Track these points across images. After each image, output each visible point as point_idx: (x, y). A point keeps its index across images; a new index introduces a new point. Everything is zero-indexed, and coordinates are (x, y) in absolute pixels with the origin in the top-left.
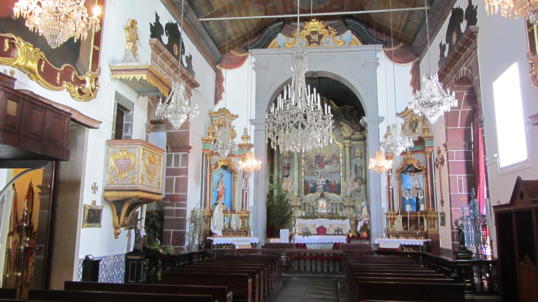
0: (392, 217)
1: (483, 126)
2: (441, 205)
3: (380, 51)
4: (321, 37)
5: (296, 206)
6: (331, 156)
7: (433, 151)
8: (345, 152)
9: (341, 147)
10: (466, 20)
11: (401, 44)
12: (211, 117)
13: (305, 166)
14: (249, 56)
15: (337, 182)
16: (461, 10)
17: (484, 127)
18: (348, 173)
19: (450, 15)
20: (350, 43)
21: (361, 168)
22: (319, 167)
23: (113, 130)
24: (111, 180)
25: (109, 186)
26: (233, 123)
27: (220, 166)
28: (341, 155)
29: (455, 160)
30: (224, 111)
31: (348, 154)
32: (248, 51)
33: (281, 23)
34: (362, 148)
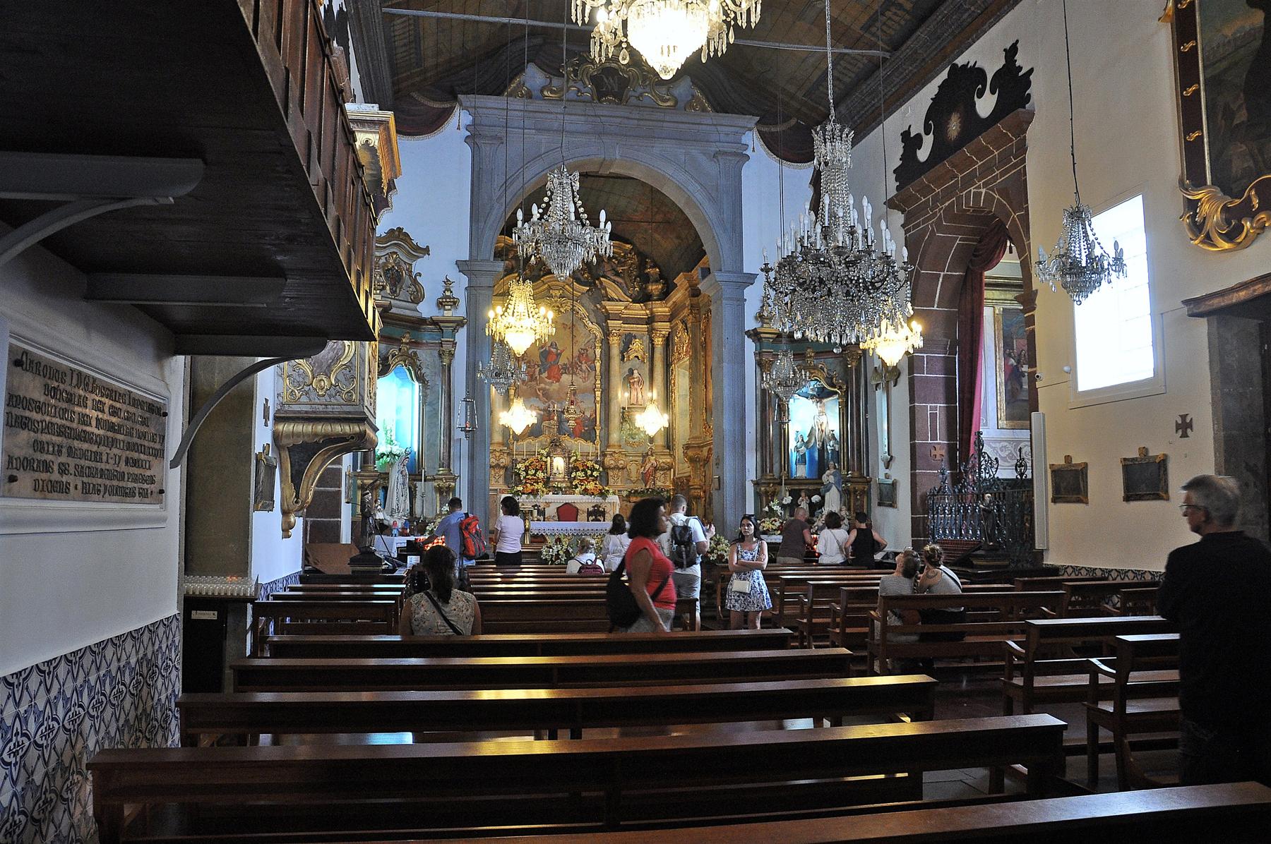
0: (771, 489)
1: (1034, 309)
2: (881, 465)
3: (750, 130)
5: (498, 466)
9: (599, 334)
10: (993, 92)
11: (793, 122)
14: (457, 110)
15: (588, 414)
16: (981, 72)
17: (1036, 313)
19: (944, 75)
20: (689, 105)
22: (549, 377)
25: (286, 407)
26: (419, 266)
28: (598, 351)
31: (615, 351)
32: (455, 98)
33: (538, 41)
34: (646, 338)
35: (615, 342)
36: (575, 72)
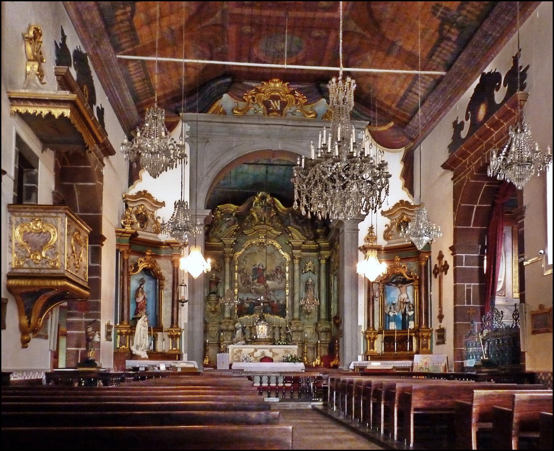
4: (284, 104)
6: (275, 269)
7: (430, 257)
8: (293, 264)
12: (126, 202)
13: (239, 280)
18: (296, 290)
21: (313, 285)
22: (258, 282)
23: (14, 190)
24: (19, 262)
27: (140, 269)
28: (287, 268)
29: (464, 266)
30: (144, 195)
34: (316, 260)
35: (296, 261)
36: (253, 99)
